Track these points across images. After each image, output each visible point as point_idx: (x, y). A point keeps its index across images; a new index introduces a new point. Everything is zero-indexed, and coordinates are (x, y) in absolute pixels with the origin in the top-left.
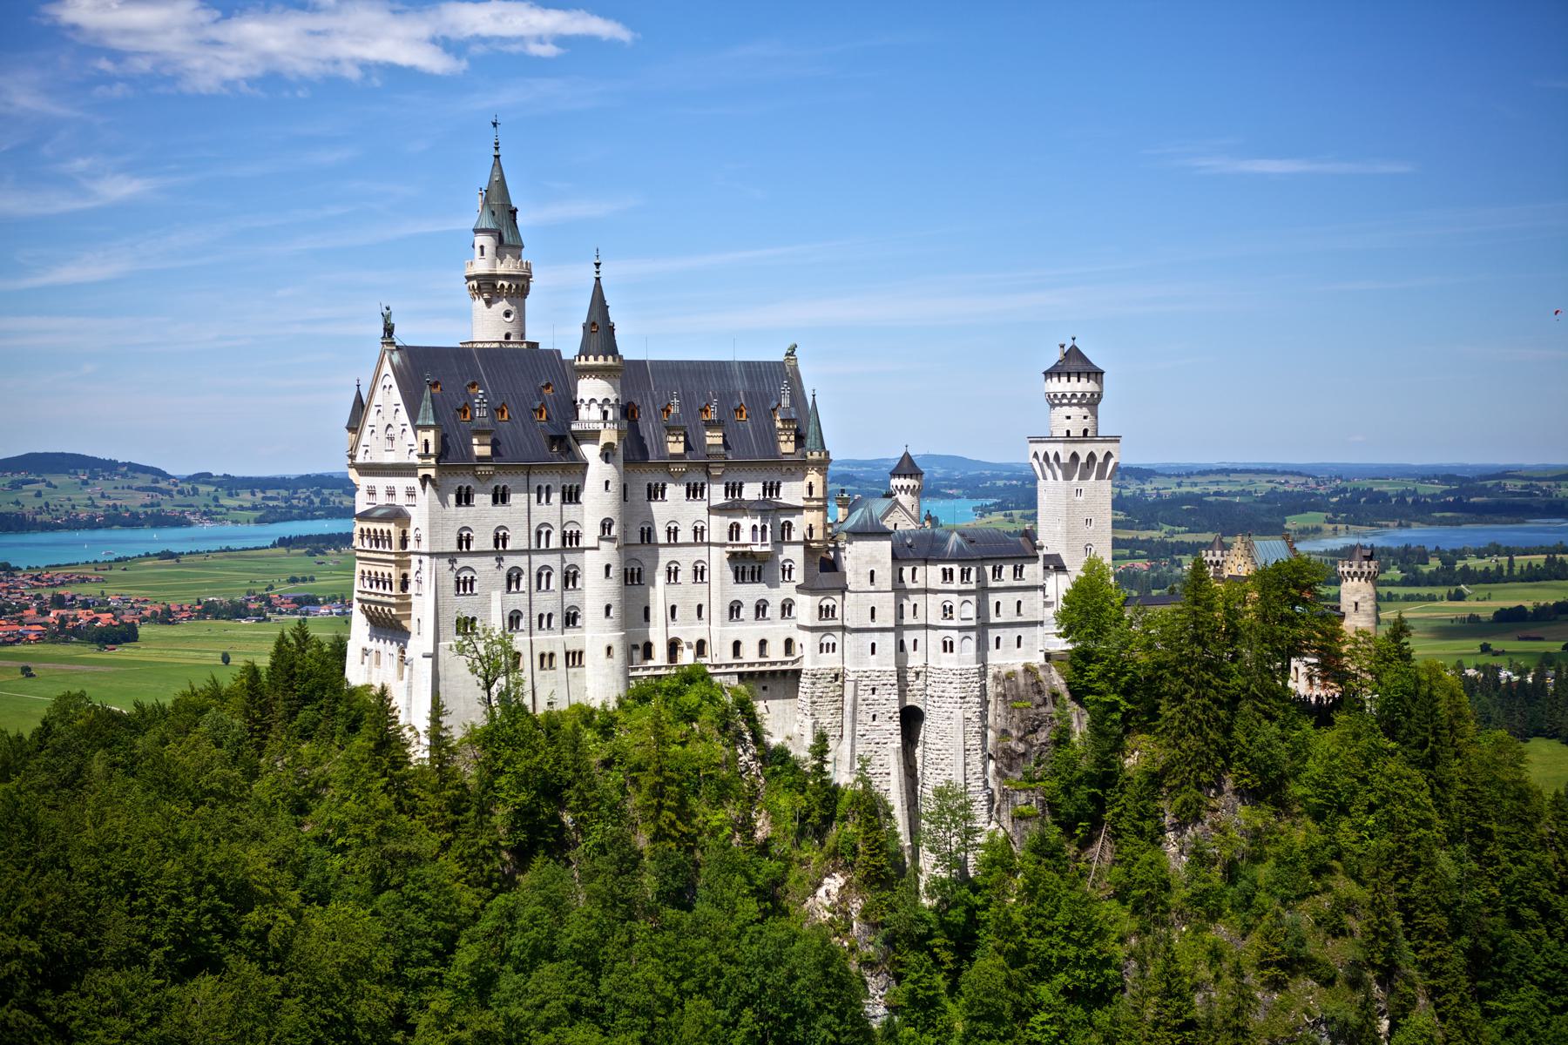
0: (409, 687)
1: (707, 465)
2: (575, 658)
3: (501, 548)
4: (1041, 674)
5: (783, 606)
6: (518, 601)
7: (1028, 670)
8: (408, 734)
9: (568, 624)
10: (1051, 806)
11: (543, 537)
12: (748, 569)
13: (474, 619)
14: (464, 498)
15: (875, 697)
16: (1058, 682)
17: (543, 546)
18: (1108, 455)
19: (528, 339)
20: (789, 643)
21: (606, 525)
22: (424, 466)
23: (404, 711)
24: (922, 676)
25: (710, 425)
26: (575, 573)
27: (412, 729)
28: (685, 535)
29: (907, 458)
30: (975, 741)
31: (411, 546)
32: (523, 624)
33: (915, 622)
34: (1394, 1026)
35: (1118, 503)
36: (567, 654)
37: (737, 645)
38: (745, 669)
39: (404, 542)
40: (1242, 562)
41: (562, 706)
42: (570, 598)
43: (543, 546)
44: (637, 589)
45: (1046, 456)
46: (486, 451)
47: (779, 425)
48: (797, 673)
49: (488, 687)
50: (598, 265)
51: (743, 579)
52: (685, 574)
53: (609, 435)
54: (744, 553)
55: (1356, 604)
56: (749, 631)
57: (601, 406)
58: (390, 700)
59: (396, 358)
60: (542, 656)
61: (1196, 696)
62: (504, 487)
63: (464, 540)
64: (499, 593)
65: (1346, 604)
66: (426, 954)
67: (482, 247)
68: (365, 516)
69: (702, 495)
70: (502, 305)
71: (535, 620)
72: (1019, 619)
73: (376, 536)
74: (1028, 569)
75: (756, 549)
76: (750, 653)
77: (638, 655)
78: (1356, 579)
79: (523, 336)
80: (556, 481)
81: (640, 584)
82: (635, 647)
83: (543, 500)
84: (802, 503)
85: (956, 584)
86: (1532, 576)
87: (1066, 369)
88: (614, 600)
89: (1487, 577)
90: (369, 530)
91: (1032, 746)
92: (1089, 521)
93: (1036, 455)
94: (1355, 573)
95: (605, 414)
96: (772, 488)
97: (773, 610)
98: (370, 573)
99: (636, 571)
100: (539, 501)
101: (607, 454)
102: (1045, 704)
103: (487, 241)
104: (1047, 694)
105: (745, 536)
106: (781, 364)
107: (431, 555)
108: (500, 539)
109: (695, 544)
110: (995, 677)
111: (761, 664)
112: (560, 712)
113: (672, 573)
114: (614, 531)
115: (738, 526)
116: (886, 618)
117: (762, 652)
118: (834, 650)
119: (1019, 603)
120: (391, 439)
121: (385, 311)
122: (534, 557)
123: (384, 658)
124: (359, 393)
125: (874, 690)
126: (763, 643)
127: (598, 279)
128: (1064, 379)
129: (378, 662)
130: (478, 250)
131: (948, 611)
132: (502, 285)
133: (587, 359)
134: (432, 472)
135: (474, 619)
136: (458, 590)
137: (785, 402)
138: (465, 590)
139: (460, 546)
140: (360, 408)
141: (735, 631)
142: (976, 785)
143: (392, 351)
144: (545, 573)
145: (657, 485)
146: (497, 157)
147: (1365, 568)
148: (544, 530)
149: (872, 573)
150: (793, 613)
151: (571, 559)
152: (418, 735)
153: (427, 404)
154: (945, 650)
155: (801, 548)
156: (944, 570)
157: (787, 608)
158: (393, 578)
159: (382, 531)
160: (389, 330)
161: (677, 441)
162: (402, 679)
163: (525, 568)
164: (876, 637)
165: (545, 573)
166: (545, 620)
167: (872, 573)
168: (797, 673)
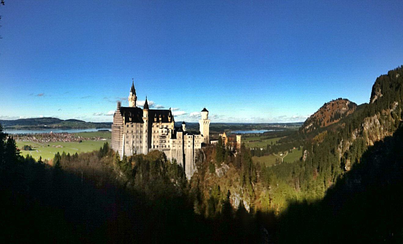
2: (141, 147)
7: (199, 149)
14: (128, 126)
20: (169, 146)
28: (156, 132)
30: (192, 158)
32: (135, 142)
42: (141, 140)
46: (131, 120)
47: (169, 118)
48: (170, 150)
49: (131, 150)
53: (147, 119)
58: (117, 152)
63: (128, 132)
65: (237, 141)
80: (139, 124)
86: (253, 136)
88: (147, 140)
89: (248, 137)
96: (167, 126)
101: (147, 121)
105: (164, 132)
108: (132, 132)
113: (154, 137)
131: (189, 142)
137: (169, 115)
142: (192, 164)
143: (119, 108)
146: (133, 83)
153: (124, 115)
157: (169, 142)
164: (180, 145)
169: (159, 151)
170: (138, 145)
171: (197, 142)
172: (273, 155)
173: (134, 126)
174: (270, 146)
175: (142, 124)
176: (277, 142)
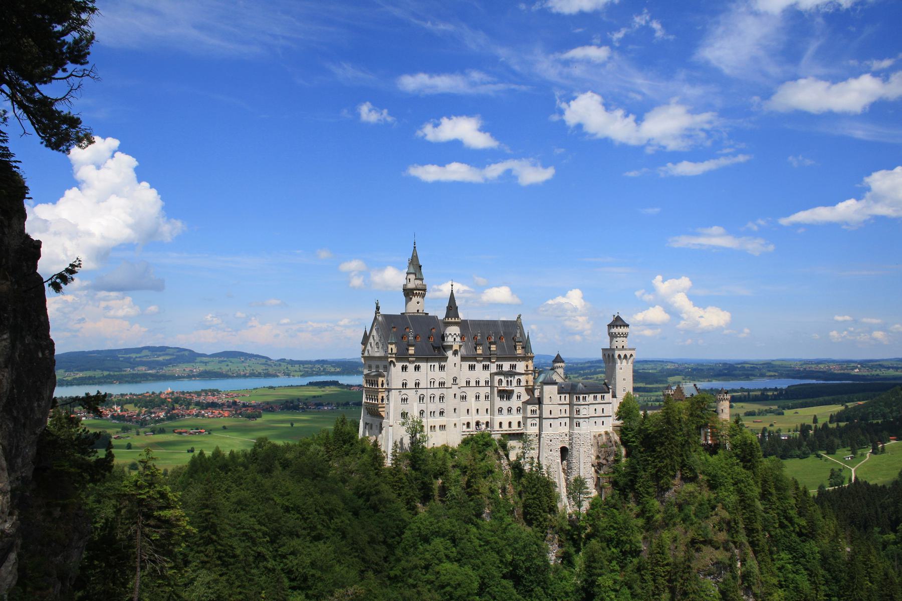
4: (611, 435)
6: (423, 406)
7: (607, 433)
8: (385, 454)
10: (615, 484)
11: (432, 383)
13: (407, 413)
14: (404, 368)
16: (616, 438)
20: (519, 423)
21: (455, 379)
22: (391, 357)
24: (568, 436)
25: (491, 343)
27: (384, 452)
28: (482, 383)
29: (558, 356)
31: (385, 386)
34: (742, 565)
35: (634, 371)
37: (501, 424)
39: (382, 385)
41: (439, 445)
50: (452, 285)
52: (482, 397)
54: (504, 390)
56: (505, 418)
57: (452, 336)
59: (380, 319)
60: (431, 427)
61: (668, 444)
63: (405, 385)
66: (394, 534)
68: (367, 375)
70: (415, 299)
72: (603, 415)
74: (606, 395)
76: (505, 426)
77: (465, 427)
82: (464, 424)
84: (524, 372)
87: (616, 324)
92: (624, 379)
95: (455, 339)
96: (513, 367)
97: (514, 411)
102: (613, 446)
103: (412, 277)
104: (613, 443)
105: (504, 384)
108: (417, 384)
109: (486, 386)
110: (594, 436)
112: (437, 448)
113: (477, 397)
115: (501, 380)
119: (603, 409)
123: (374, 427)
125: (551, 441)
126: (510, 423)
129: (371, 428)
134: (394, 360)
135: (407, 413)
137: (518, 335)
146: (415, 247)
148: (432, 381)
151: (444, 391)
152: (387, 455)
155: (524, 388)
160: (378, 308)
161: (479, 349)
163: (425, 395)
166: (432, 413)
168: (522, 434)
169: (493, 436)
172: (822, 456)
174: (809, 427)
175: (443, 364)
176: (831, 417)
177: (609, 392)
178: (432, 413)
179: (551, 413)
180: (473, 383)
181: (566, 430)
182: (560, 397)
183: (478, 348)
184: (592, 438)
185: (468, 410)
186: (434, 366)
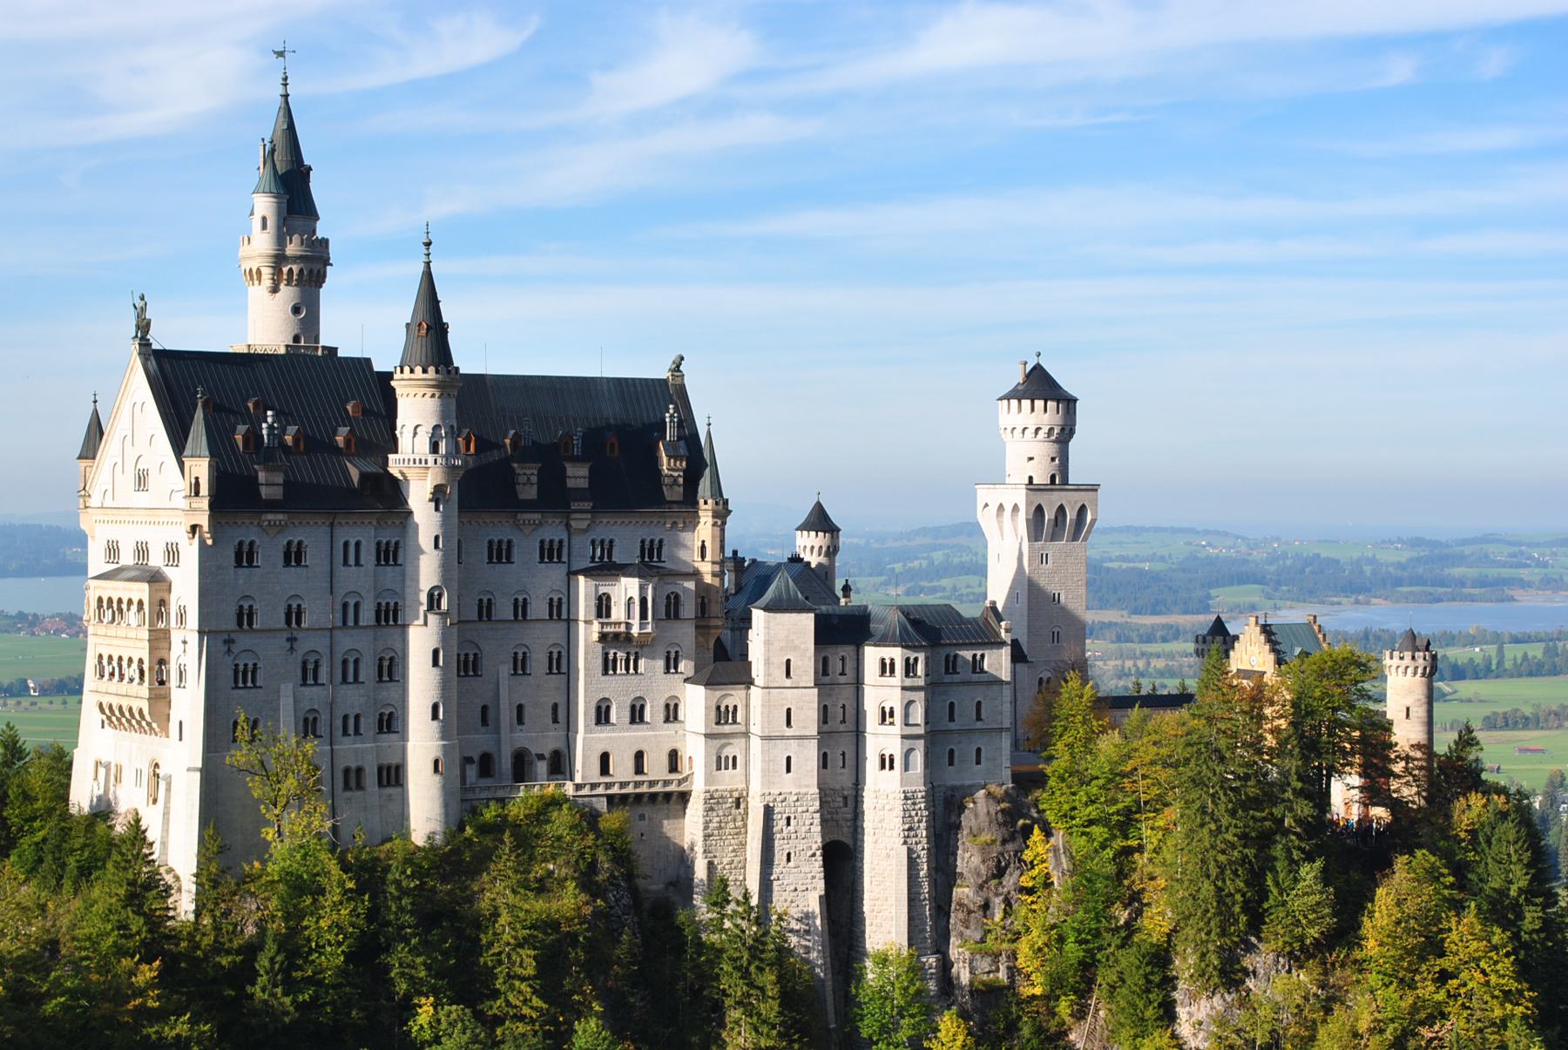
0: (166, 814)
1: (568, 519)
2: (393, 776)
3: (294, 625)
5: (667, 706)
8: (169, 879)
9: (381, 731)
12: (621, 655)
14: (245, 556)
15: (791, 828)
17: (351, 623)
18: (1082, 510)
19: (325, 340)
23: (156, 847)
26: (391, 659)
27: (170, 870)
28: (538, 609)
32: (323, 728)
33: (842, 728)
36: (380, 769)
37: (605, 758)
38: (615, 790)
40: (1255, 649)
43: (351, 623)
44: (473, 682)
45: (1001, 507)
48: (684, 797)
50: (428, 244)
51: (615, 669)
52: (538, 662)
54: (617, 635)
55: (1408, 709)
56: (621, 740)
58: (146, 830)
59: (153, 364)
60: (347, 771)
62: (300, 543)
63: (245, 617)
64: (290, 686)
65: (1393, 709)
67: (264, 219)
69: (559, 557)
71: (339, 723)
72: (979, 725)
73: (120, 610)
75: (635, 631)
76: (622, 769)
77: (472, 771)
78: (1410, 671)
79: (317, 340)
81: (476, 675)
83: (352, 560)
85: (899, 677)
90: (110, 600)
91: (997, 895)
93: (986, 505)
94: (1407, 667)
98: (110, 658)
99: (471, 658)
100: (346, 563)
101: (438, 496)
105: (618, 613)
106: (665, 381)
107: (201, 632)
108: (293, 615)
111: (637, 784)
114: (444, 605)
116: (807, 719)
117: (639, 769)
118: (734, 766)
120: (142, 480)
121: (139, 304)
122: (337, 633)
123: (128, 776)
124: (96, 413)
125: (788, 819)
126: (639, 756)
127: (428, 264)
128: (1026, 403)
129: (118, 779)
130: (256, 222)
131: (885, 716)
132: (291, 271)
133: (412, 371)
134: (203, 521)
136: (236, 681)
138: (245, 681)
139: (240, 624)
140: (96, 432)
141: (604, 738)
144: (351, 660)
145: (500, 542)
147: (1421, 662)
148: (352, 603)
149: (788, 662)
150: (681, 716)
152: (177, 878)
154: (883, 767)
156: (883, 660)
157: (671, 713)
158: (146, 667)
159: (130, 602)
160: (143, 327)
162: (155, 801)
164: (792, 748)
165: (351, 660)
166: (350, 726)
167: (788, 662)
170: (361, 751)
171: (965, 716)
173: (308, 559)
177: (1003, 643)
178: (351, 722)
179: (789, 723)
180: (504, 610)
181: (845, 779)
182: (825, 661)
183: (522, 479)
184: (940, 809)
185: (484, 709)
186: (358, 544)
